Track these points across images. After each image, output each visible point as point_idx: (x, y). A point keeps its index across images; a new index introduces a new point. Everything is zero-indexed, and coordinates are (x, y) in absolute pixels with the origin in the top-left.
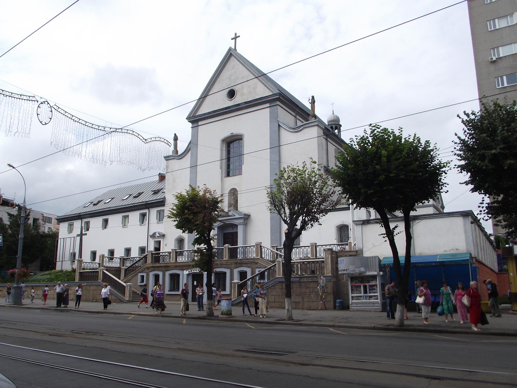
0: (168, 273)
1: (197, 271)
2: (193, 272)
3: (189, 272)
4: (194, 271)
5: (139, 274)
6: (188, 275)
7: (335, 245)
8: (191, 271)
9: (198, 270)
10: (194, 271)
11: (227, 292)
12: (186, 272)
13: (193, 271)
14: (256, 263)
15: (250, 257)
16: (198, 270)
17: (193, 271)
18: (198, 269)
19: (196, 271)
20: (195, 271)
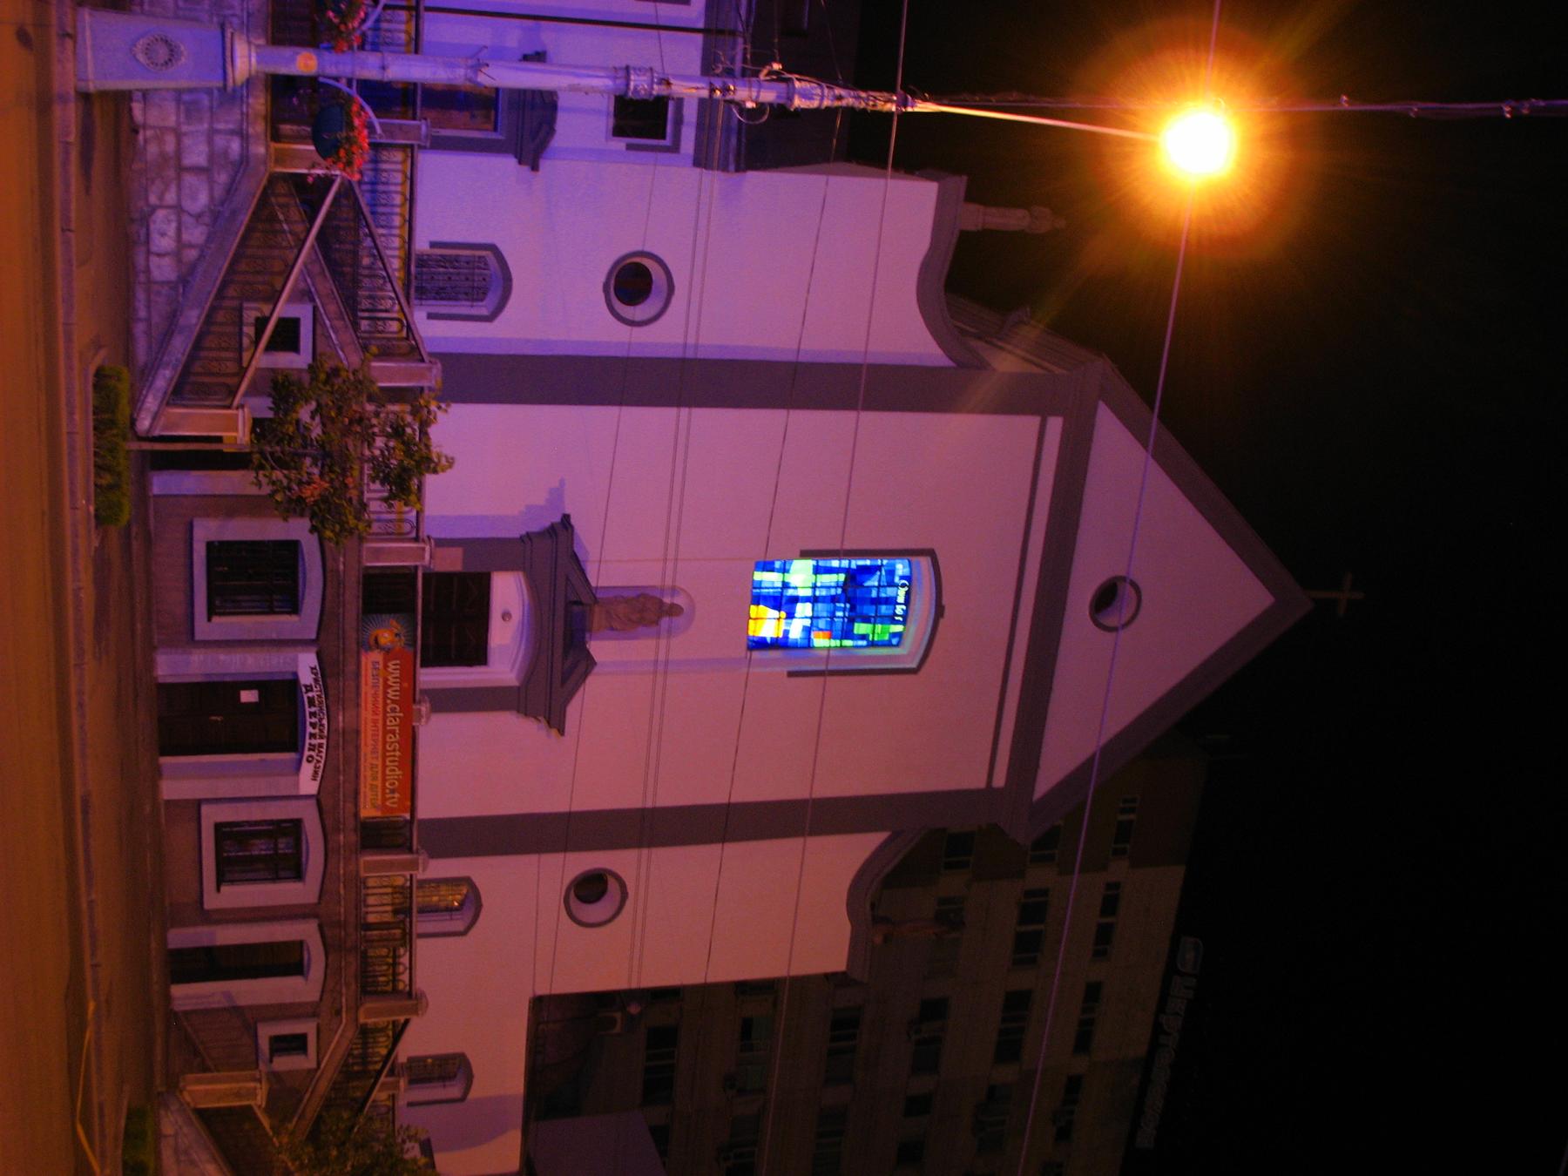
0: (298, 529)
1: (312, 736)
2: (308, 710)
3: (309, 688)
4: (313, 720)
5: (310, 307)
6: (295, 674)
7: (394, 1113)
8: (311, 702)
9: (314, 742)
10: (313, 720)
11: (212, 901)
12: (305, 665)
13: (313, 714)
14: (339, 1013)
15: (365, 901)
16: (314, 742)
17: (313, 714)
18: (320, 745)
19: (310, 730)
20: (313, 725)
